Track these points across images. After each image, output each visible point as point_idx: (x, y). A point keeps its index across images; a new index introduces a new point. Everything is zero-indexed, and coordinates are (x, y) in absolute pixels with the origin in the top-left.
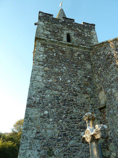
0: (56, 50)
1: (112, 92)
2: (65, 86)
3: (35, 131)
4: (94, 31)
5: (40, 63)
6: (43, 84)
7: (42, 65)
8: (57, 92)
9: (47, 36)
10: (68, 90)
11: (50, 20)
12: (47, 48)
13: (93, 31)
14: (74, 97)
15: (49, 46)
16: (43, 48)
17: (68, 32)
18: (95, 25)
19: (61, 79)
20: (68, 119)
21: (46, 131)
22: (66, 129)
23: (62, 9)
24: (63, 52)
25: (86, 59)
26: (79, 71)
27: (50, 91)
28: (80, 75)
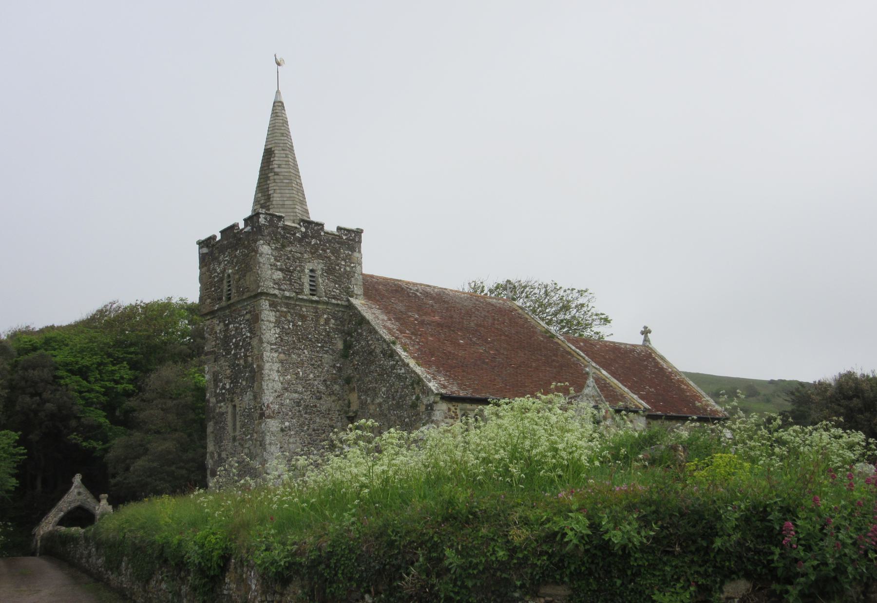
0: (292, 315)
1: (367, 401)
2: (308, 385)
3: (278, 446)
4: (360, 252)
5: (272, 347)
6: (280, 384)
7: (275, 352)
8: (296, 395)
10: (311, 391)
11: (280, 233)
12: (278, 311)
13: (356, 254)
15: (281, 307)
16: (273, 313)
17: (311, 268)
18: (362, 231)
19: (301, 373)
20: (310, 430)
21: (288, 445)
23: (282, 103)
24: (303, 318)
25: (337, 328)
26: (326, 356)
27: (289, 394)
28: (327, 363)
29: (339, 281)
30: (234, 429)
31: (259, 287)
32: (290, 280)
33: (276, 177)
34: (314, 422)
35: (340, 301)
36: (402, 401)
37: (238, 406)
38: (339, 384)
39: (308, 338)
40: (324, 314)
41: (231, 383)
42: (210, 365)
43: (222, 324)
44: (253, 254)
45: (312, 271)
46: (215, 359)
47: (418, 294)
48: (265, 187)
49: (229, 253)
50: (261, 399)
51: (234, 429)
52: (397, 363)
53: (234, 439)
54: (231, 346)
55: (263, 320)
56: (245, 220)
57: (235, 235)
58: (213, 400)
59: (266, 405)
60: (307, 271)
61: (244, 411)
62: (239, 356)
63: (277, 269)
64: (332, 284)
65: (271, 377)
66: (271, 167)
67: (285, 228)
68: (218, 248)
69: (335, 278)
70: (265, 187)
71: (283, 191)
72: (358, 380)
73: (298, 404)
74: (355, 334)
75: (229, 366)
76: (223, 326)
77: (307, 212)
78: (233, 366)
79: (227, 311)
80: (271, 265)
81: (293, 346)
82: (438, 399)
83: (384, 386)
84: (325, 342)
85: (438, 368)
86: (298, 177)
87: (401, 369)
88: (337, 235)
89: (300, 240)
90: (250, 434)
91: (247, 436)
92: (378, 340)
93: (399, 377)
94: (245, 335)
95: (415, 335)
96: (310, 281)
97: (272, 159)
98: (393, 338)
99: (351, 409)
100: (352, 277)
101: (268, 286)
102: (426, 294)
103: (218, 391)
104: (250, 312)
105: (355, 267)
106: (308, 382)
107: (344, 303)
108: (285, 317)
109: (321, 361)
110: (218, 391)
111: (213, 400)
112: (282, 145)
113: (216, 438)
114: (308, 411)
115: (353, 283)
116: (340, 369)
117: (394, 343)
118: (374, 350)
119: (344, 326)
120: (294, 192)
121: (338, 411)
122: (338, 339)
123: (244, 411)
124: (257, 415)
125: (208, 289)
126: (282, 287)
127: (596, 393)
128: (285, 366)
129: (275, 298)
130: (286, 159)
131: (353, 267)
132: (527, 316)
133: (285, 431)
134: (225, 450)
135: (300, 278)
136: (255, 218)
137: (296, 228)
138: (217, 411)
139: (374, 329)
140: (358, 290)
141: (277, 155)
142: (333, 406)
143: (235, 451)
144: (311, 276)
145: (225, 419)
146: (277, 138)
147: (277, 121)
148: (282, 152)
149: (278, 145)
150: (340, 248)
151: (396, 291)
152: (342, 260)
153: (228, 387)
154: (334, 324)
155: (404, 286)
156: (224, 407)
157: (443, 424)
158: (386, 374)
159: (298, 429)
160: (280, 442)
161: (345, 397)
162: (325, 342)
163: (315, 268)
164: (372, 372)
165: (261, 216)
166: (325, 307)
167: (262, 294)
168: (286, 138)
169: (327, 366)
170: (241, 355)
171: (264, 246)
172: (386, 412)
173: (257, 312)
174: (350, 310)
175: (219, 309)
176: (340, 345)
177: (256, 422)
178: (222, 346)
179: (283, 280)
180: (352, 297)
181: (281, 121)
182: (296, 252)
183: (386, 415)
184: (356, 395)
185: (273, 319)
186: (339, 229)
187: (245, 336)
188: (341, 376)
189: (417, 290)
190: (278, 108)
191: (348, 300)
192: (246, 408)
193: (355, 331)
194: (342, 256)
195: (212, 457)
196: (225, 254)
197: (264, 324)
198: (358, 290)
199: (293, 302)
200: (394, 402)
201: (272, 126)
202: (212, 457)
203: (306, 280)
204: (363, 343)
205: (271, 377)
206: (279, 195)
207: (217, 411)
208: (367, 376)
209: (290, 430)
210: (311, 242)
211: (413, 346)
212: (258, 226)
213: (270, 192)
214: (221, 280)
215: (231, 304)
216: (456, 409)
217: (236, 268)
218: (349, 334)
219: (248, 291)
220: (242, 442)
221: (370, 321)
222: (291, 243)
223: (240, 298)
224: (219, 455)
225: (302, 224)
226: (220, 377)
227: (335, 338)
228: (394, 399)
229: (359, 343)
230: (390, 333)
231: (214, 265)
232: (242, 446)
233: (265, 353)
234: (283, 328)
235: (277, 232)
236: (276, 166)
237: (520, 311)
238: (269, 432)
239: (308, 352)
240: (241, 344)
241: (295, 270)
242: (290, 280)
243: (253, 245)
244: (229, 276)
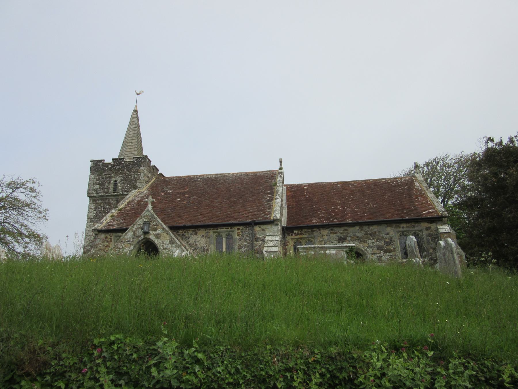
0: (103, 204)
9: (96, 191)
16: (94, 205)
45: (116, 181)
80: (94, 183)
89: (110, 169)
100: (138, 179)
126: (98, 192)
150: (132, 167)
152: (133, 172)
182: (108, 175)
185: (93, 207)
190: (136, 111)
203: (111, 187)
205: (88, 234)
216: (111, 237)
222: (105, 171)
234: (98, 210)
242: (103, 188)
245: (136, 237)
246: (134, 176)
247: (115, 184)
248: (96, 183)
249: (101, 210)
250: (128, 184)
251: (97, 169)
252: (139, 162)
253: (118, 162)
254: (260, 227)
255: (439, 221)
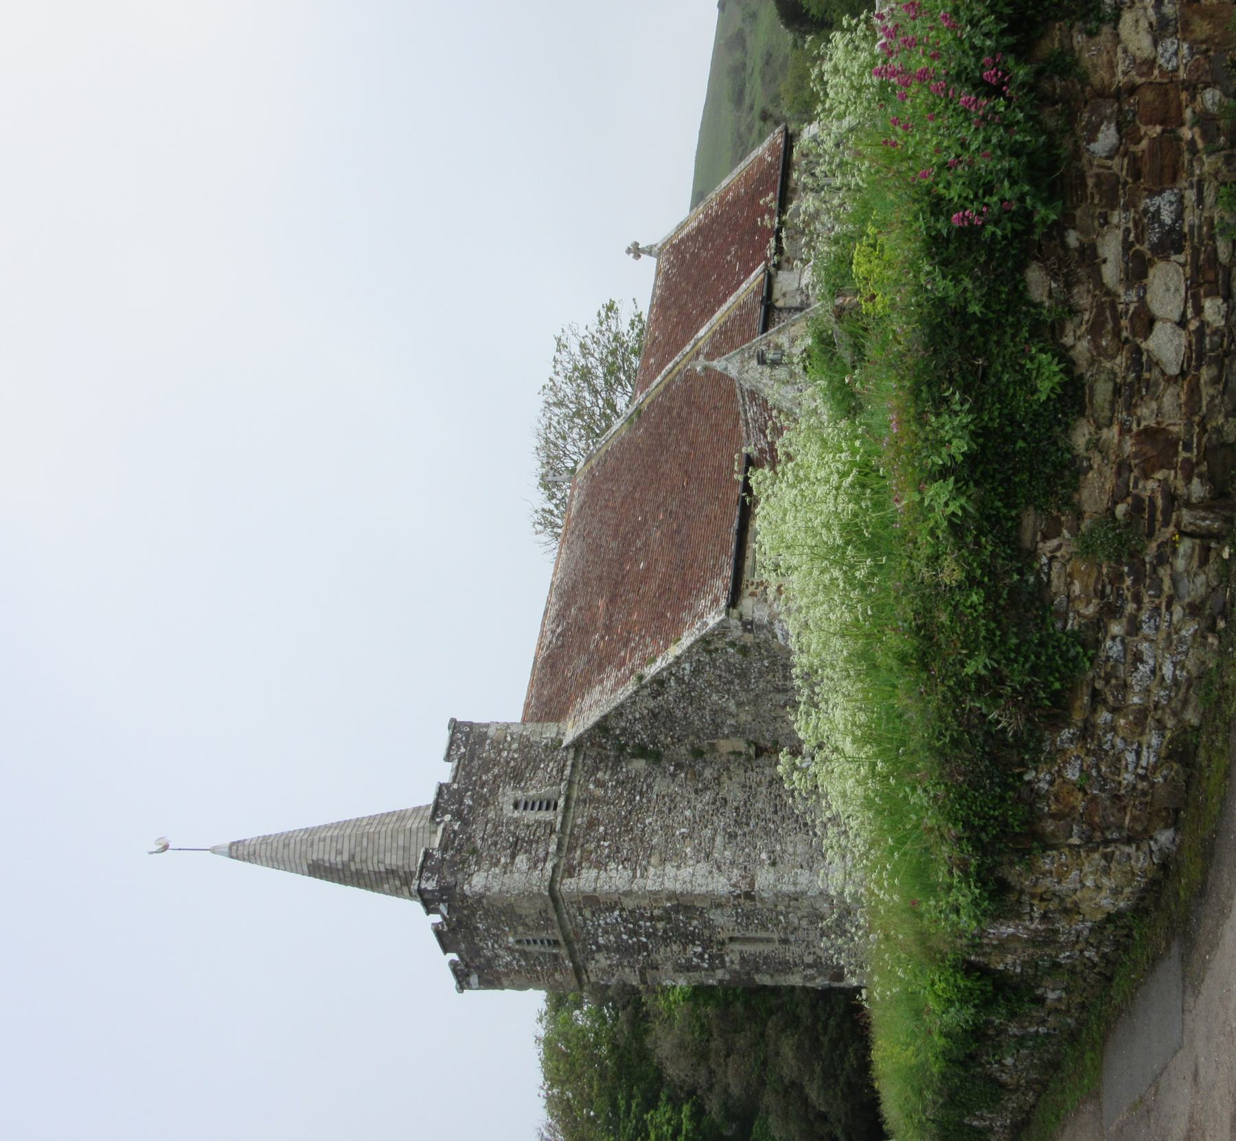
0: (587, 842)
2: (702, 820)
3: (799, 871)
4: (487, 726)
5: (638, 875)
8: (719, 839)
11: (453, 856)
12: (580, 864)
13: (491, 732)
14: (729, 804)
15: (574, 859)
16: (584, 871)
17: (512, 807)
18: (453, 721)
19: (683, 830)
22: (797, 821)
23: (233, 844)
24: (592, 824)
25: (612, 769)
26: (656, 788)
27: (715, 850)
28: (669, 787)
29: (535, 761)
30: (769, 940)
31: (540, 895)
32: (530, 842)
33: (357, 859)
34: (763, 811)
35: (565, 761)
36: (736, 668)
37: (731, 934)
38: (704, 768)
39: (625, 817)
40: (587, 789)
41: (694, 944)
42: (663, 978)
43: (597, 956)
44: (485, 901)
45: (516, 806)
46: (653, 968)
47: (559, 630)
48: (373, 878)
49: (481, 940)
50: (722, 896)
51: (769, 940)
52: (674, 675)
53: (785, 941)
54: (634, 943)
55: (595, 890)
56: (428, 912)
57: (453, 930)
58: (720, 974)
59: (732, 889)
60: (516, 814)
61: (740, 924)
62: (651, 930)
63: (512, 863)
64: (540, 773)
65: (687, 879)
66: (340, 867)
67: (444, 848)
68: (471, 958)
69: (530, 767)
70: (373, 878)
71: (382, 849)
72: (698, 737)
73: (733, 836)
74: (623, 740)
75: (667, 946)
76: (601, 954)
77: (417, 810)
78: (666, 940)
79: (576, 947)
80: (505, 873)
81: (638, 841)
82: (735, 613)
83: (710, 697)
84: (634, 788)
85: (684, 608)
86: (358, 823)
87: (684, 669)
88: (459, 762)
89: (466, 823)
90: (777, 915)
91: (780, 921)
92: (634, 703)
93: (696, 672)
94: (616, 919)
95: (628, 641)
96: (532, 808)
97: (327, 864)
98: (633, 679)
99: (743, 750)
100: (529, 739)
101: (538, 880)
102: (561, 616)
103: (706, 965)
104: (580, 909)
105: (511, 735)
106: (698, 820)
107: (571, 755)
108: (591, 853)
109: (664, 797)
110: (706, 965)
111: (720, 974)
112: (304, 848)
113: (782, 971)
114: (744, 820)
115: (538, 739)
116: (679, 766)
117: (641, 678)
118: (651, 711)
119: (608, 757)
120: (384, 829)
121: (745, 772)
122: (630, 767)
123: (740, 924)
124: (748, 904)
125: (538, 977)
126: (542, 855)
127: (738, 357)
128: (670, 855)
129: (559, 868)
130: (328, 841)
131: (512, 738)
132: (603, 450)
133: (775, 859)
134: (801, 957)
135: (528, 826)
136: (426, 896)
137: (444, 829)
138: (737, 967)
139: (616, 708)
140: (550, 731)
141: (321, 856)
142: (738, 780)
143: (804, 941)
144: (525, 808)
145: (751, 954)
146: (291, 855)
147: (262, 854)
148: (315, 847)
149: (303, 854)
150: (479, 758)
151: (553, 666)
152: (499, 754)
153: (699, 949)
154: (605, 773)
155: (544, 653)
156: (732, 956)
157: (775, 606)
158: (690, 692)
159: (773, 839)
160: (793, 867)
161: (724, 759)
162: (634, 788)
163: (512, 801)
164: (685, 714)
165: (423, 887)
166: (576, 786)
167: (551, 889)
168: (292, 841)
169: (672, 787)
170: (648, 927)
171: (474, 882)
172: (752, 696)
173: (580, 899)
174: (582, 746)
175: (572, 956)
176: (639, 764)
177: (759, 905)
178: (632, 957)
179: (531, 853)
180: (561, 742)
181: (263, 847)
182: (485, 831)
183: (757, 695)
184: (721, 741)
185: (594, 873)
186: (448, 758)
187: (619, 919)
188: (690, 765)
189: (553, 632)
190: (239, 851)
191: (567, 748)
192: (736, 921)
193: (618, 739)
194: (492, 755)
195: (813, 978)
196: (482, 948)
197: (602, 887)
198: (550, 731)
199: (567, 839)
200: (737, 681)
201: (270, 863)
202: (813, 978)
203: (531, 816)
204: (638, 727)
205: (687, 879)
206: (388, 855)
207: (737, 967)
208: (692, 723)
209: (773, 852)
210: (469, 806)
211: (647, 646)
212: (438, 891)
213: (382, 869)
214: (524, 954)
215: (565, 940)
217: (507, 929)
218: (621, 748)
219: (546, 911)
220: (791, 928)
221: (603, 714)
222: (469, 839)
223: (557, 925)
224: (809, 966)
225: (438, 820)
226: (683, 961)
227: (627, 772)
228: (732, 682)
229: (638, 733)
230: (624, 683)
231: (499, 965)
232: (795, 929)
233: (647, 888)
234: (608, 856)
235: (450, 861)
236: (339, 858)
237: (593, 462)
238: (776, 886)
239: (648, 817)
240: (631, 926)
241: (515, 833)
242: (530, 842)
243: (470, 901)
244: (519, 942)
245: (791, 377)
246: (515, 751)
247: (528, 805)
248: (505, 866)
249: (609, 846)
250: (536, 768)
251: (456, 864)
252: (467, 739)
253: (448, 800)
254: (777, 300)
255: (792, 141)
